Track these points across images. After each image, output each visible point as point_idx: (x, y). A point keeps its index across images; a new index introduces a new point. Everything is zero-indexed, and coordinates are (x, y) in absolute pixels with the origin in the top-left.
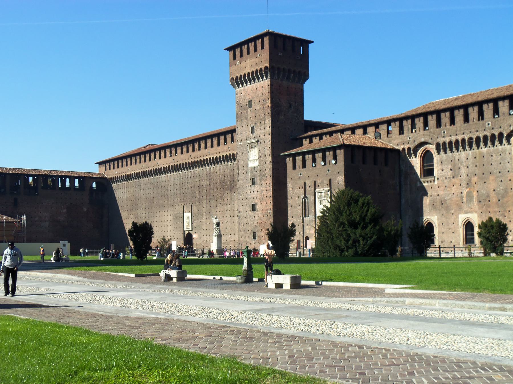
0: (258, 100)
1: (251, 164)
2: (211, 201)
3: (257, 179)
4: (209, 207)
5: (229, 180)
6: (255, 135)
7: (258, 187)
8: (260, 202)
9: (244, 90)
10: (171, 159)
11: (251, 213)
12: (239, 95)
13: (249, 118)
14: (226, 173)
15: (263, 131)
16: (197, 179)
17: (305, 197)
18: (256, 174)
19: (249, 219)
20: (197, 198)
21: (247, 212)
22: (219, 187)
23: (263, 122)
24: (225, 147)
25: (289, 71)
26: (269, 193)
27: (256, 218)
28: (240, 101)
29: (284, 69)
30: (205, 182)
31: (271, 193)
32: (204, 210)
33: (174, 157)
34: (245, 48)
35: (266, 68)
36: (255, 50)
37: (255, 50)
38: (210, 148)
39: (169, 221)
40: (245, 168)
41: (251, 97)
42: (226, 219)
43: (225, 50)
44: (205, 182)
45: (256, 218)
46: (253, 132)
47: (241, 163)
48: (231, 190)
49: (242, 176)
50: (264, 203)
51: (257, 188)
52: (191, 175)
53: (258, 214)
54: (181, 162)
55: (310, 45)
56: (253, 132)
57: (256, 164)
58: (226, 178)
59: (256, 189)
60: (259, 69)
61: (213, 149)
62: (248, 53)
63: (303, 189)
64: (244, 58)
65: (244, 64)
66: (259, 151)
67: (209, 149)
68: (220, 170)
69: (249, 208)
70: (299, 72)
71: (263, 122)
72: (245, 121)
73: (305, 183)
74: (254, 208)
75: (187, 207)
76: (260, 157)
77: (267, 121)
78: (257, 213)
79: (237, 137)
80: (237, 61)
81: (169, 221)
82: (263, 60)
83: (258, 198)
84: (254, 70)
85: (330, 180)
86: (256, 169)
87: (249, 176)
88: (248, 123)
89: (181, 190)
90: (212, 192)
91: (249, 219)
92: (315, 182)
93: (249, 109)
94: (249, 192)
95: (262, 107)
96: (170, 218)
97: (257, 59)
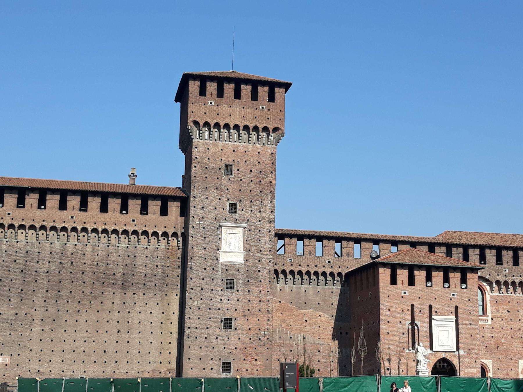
0: (249, 168)
1: (224, 258)
3: (239, 282)
4: (52, 310)
5: (120, 270)
6: (237, 216)
7: (241, 295)
13: (224, 188)
14: (113, 259)
15: (257, 214)
17: (413, 324)
19: (214, 341)
20: (13, 292)
21: (210, 330)
22: (89, 280)
23: (258, 202)
26: (265, 306)
32: (38, 315)
40: (209, 261)
42: (106, 335)
45: (234, 340)
50: (253, 319)
51: (233, 295)
53: (239, 335)
57: (239, 259)
58: (112, 267)
59: (235, 297)
63: (410, 312)
65: (224, 108)
68: (93, 251)
71: (258, 202)
73: (412, 306)
74: (228, 323)
76: (248, 251)
78: (236, 332)
82: (271, 117)
83: (240, 309)
85: (456, 308)
87: (220, 273)
88: (221, 195)
90: (66, 285)
91: (214, 341)
92: (430, 307)
93: (225, 178)
94: (217, 299)
95: (258, 180)
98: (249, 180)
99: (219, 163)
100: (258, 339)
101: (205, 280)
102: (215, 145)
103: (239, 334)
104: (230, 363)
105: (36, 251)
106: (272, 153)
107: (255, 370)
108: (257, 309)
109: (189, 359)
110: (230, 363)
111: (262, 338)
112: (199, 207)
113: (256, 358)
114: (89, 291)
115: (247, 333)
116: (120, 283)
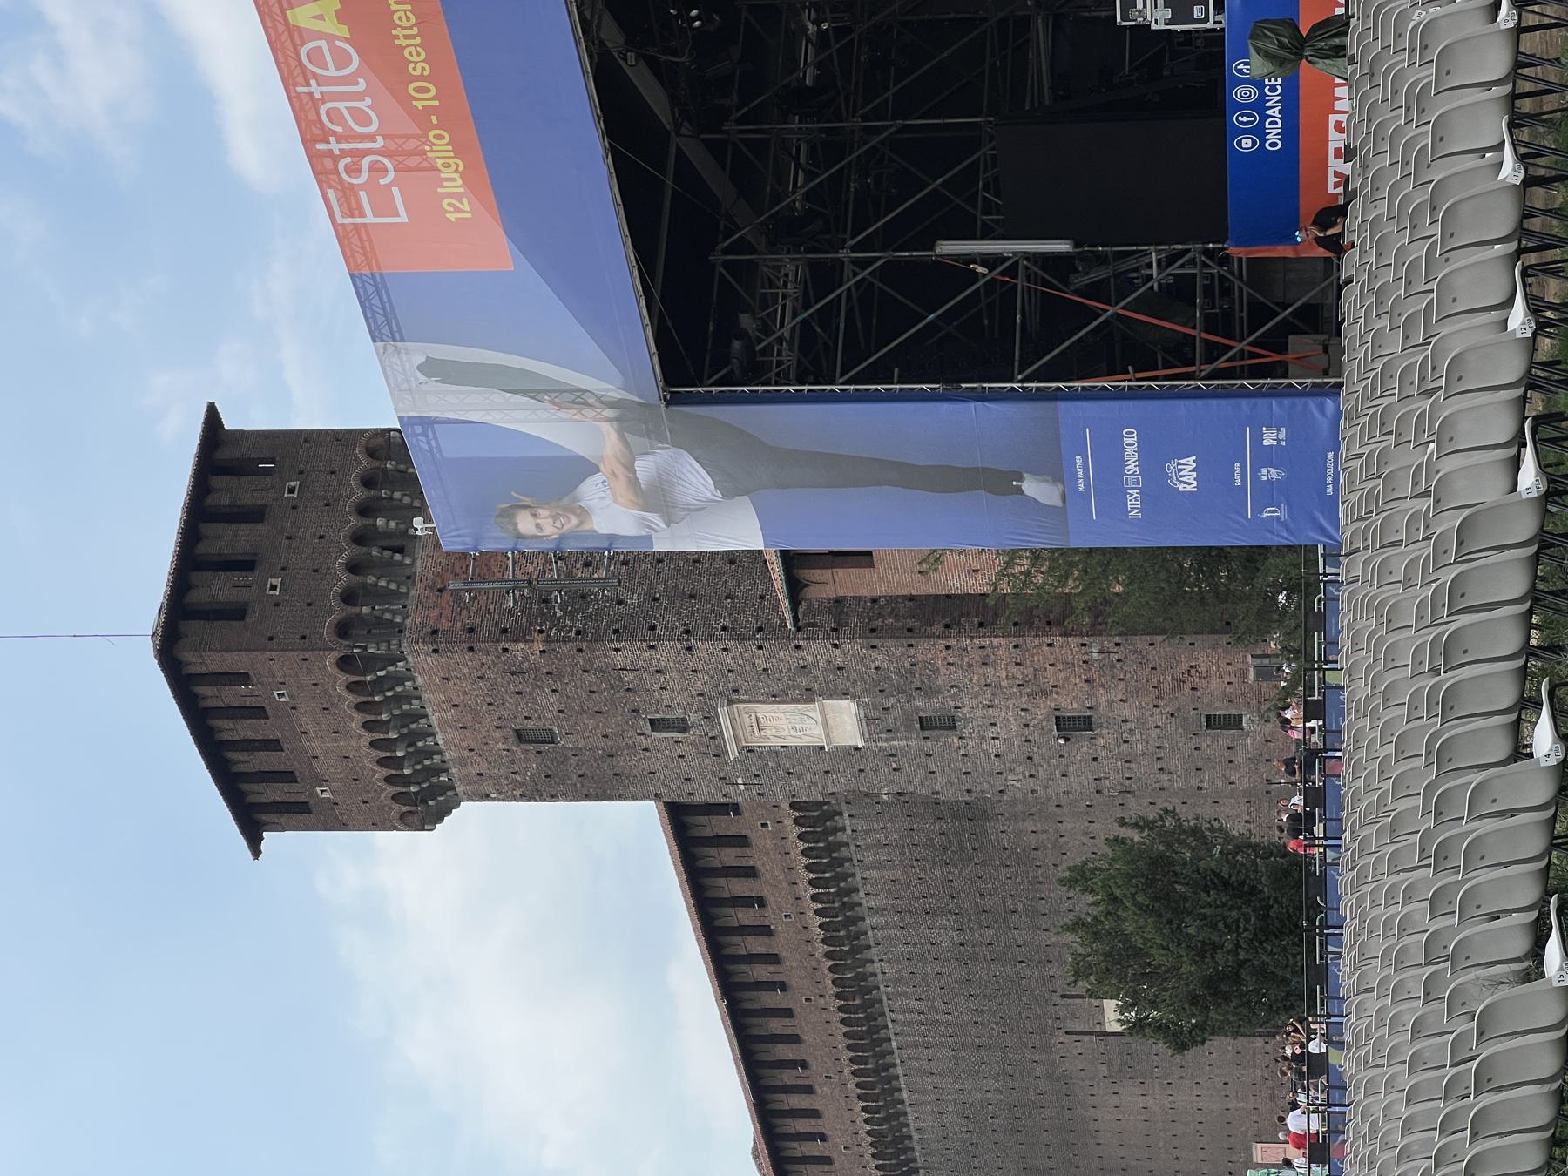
2: (1042, 906)
6: (693, 717)
8: (1044, 692)
9: (462, 762)
10: (823, 1089)
11: (1105, 738)
12: (488, 787)
15: (671, 678)
16: (931, 969)
18: (897, 712)
23: (628, 677)
24: (762, 841)
25: (358, 539)
27: (1130, 711)
28: (521, 784)
29: (353, 568)
30: (946, 934)
31: (1001, 645)
33: (815, 1075)
34: (248, 762)
35: (345, 663)
36: (259, 712)
37: (259, 712)
38: (768, 912)
39: (1149, 1101)
41: (498, 734)
43: (256, 852)
44: (946, 934)
45: (1130, 711)
46: (682, 726)
47: (839, 784)
48: (986, 817)
49: (913, 780)
52: (905, 995)
53: (1109, 703)
54: (841, 1042)
55: (229, 425)
56: (682, 726)
60: (352, 699)
61: (770, 899)
62: (274, 745)
64: (296, 767)
66: (775, 697)
67: (773, 916)
68: (879, 866)
69: (1081, 748)
70: (368, 482)
72: (623, 762)
75: (1074, 1017)
76: (809, 696)
77: (619, 659)
78: (1103, 707)
79: (705, 793)
80: (313, 795)
81: (1149, 1101)
82: (306, 679)
84: (359, 718)
86: (875, 714)
87: (907, 743)
88: (632, 748)
89: (983, 1041)
94: (993, 747)
96: (1130, 1095)
97: (302, 708)
98: (553, 698)
99: (519, 755)
100: (1118, 665)
101: (933, 768)
102: (462, 762)
103: (1107, 701)
104: (1208, 717)
105: (901, 948)
106: (436, 651)
107: (1229, 668)
108: (1014, 669)
109: (1200, 788)
110: (1208, 717)
111: (1115, 657)
112: (688, 787)
113: (1184, 668)
114: (1003, 870)
115: (1103, 686)
116: (969, 824)
